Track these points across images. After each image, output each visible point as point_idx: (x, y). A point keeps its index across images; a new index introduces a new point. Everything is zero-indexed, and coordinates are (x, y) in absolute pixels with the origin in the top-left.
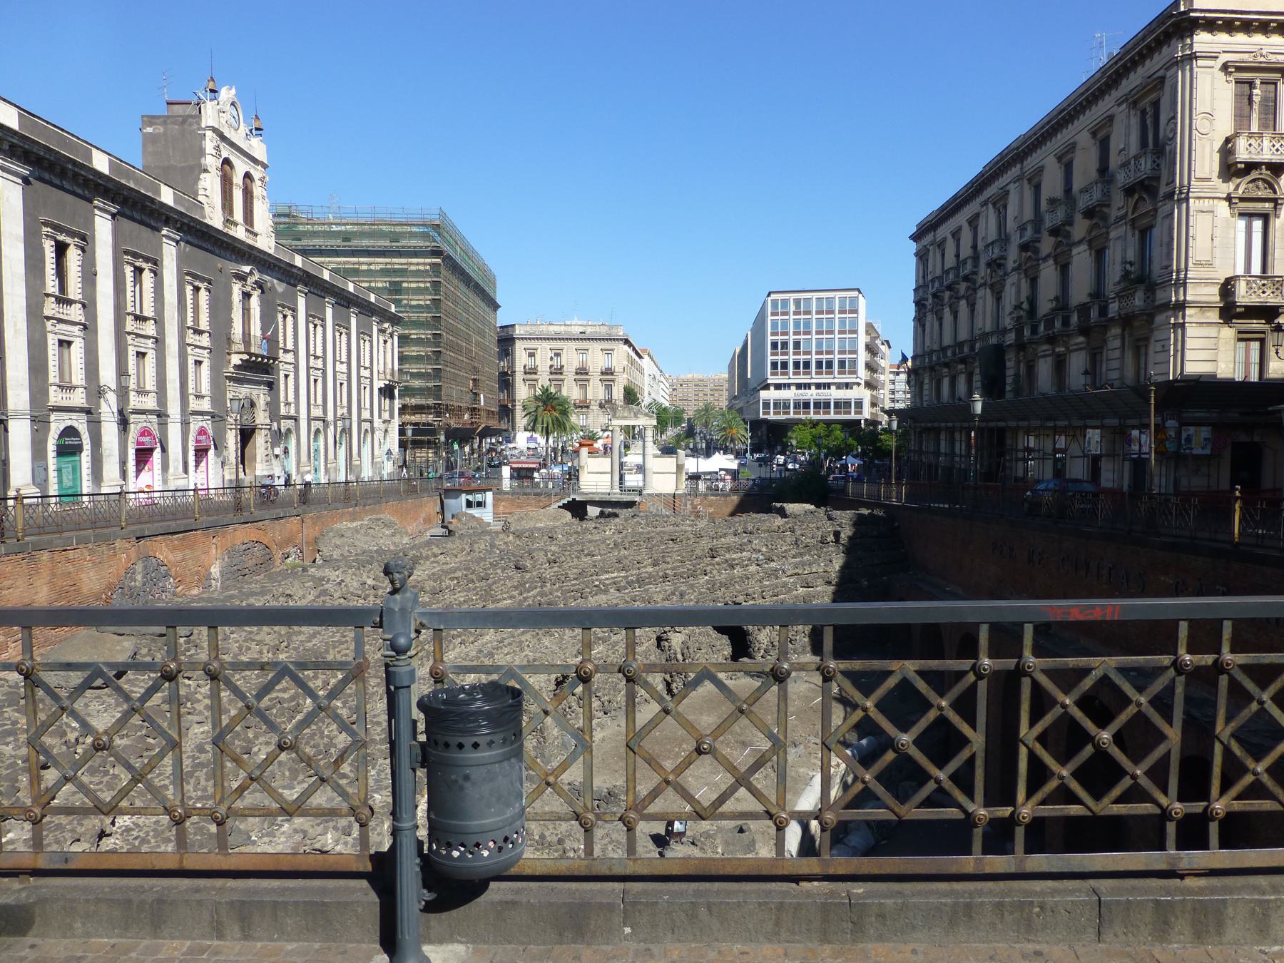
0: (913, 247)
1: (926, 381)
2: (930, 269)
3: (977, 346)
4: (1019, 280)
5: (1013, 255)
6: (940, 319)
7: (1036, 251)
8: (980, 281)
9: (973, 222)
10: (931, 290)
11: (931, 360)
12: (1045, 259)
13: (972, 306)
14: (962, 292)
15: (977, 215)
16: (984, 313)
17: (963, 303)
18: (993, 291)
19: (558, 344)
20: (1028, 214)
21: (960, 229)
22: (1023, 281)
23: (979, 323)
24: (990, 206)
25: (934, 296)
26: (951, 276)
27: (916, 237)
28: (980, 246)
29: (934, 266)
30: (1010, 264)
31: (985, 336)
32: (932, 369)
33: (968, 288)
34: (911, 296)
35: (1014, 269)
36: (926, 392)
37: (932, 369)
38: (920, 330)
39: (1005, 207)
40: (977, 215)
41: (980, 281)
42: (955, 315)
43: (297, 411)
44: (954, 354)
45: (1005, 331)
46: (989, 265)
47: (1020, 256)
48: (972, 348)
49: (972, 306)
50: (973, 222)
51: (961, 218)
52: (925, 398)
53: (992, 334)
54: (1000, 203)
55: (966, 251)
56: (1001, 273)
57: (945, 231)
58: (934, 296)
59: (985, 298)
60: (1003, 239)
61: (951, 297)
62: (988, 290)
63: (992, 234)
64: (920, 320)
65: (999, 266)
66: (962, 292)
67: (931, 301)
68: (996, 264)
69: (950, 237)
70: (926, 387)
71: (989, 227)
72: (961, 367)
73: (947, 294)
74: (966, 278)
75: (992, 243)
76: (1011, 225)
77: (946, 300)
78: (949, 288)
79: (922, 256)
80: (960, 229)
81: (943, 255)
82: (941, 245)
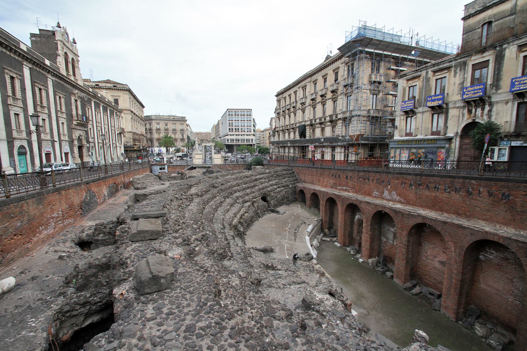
0: (276, 98)
5: (308, 101)
6: (285, 118)
8: (297, 108)
12: (318, 103)
13: (295, 115)
20: (313, 91)
27: (277, 96)
30: (307, 104)
32: (283, 130)
37: (283, 130)
42: (290, 117)
49: (295, 115)
50: (295, 92)
51: (292, 91)
54: (304, 88)
55: (293, 100)
57: (286, 94)
59: (299, 113)
65: (304, 104)
72: (292, 130)
74: (294, 107)
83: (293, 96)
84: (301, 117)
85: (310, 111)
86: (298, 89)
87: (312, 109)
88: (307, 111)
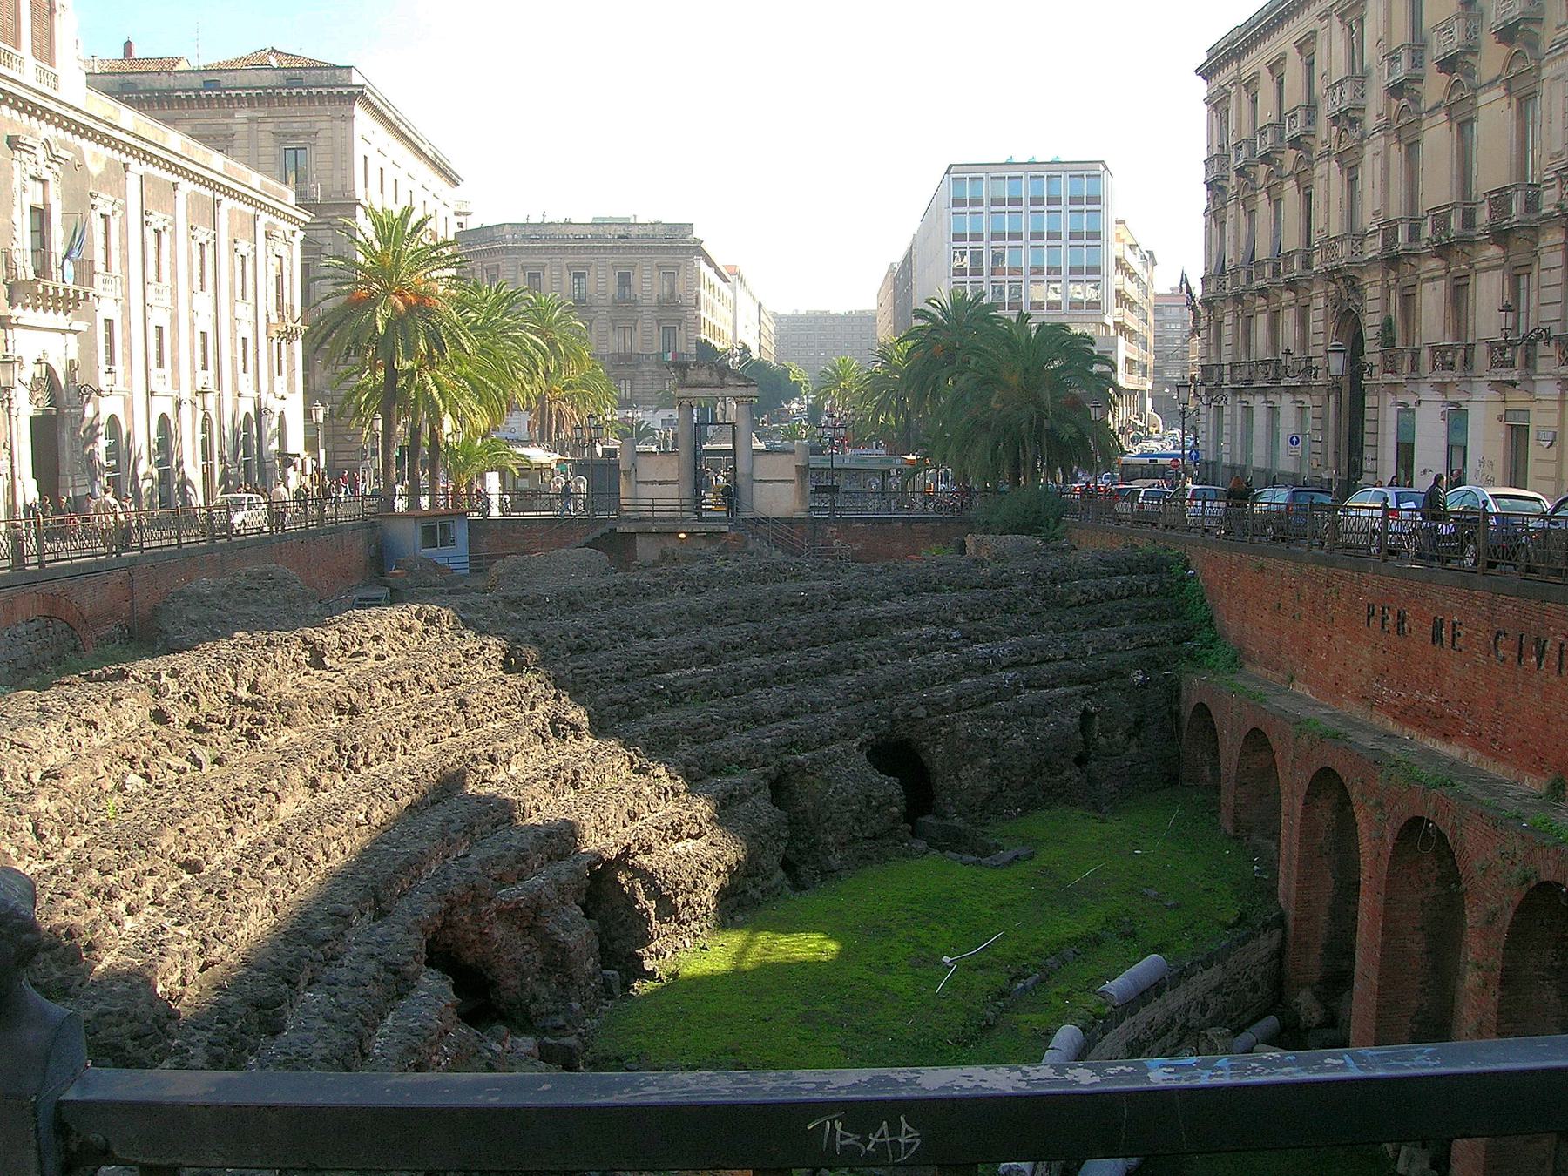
0: (1201, 88)
1: (1228, 320)
2: (1232, 126)
3: (1316, 259)
4: (1387, 148)
5: (1376, 103)
6: (1251, 213)
7: (1416, 100)
9: (1306, 45)
10: (1234, 163)
11: (1235, 283)
14: (1288, 167)
15: (1313, 34)
16: (1328, 202)
17: (1290, 185)
18: (1341, 165)
19: (584, 258)
20: (1401, 35)
21: (1282, 58)
22: (1395, 148)
23: (1318, 223)
24: (1335, 19)
25: (1240, 172)
26: (1269, 138)
27: (1206, 72)
28: (1319, 88)
29: (1239, 120)
30: (1371, 121)
31: (1328, 244)
33: (1299, 160)
34: (1199, 174)
35: (1379, 128)
36: (1226, 340)
37: (1238, 298)
38: (1215, 231)
39: (1361, 21)
40: (1313, 34)
41: (1319, 148)
43: (130, 384)
44: (1276, 273)
45: (1362, 237)
46: (1335, 120)
47: (1389, 105)
48: (1307, 265)
50: (1306, 45)
51: (1285, 41)
52: (1225, 350)
53: (1341, 239)
55: (1294, 96)
56: (1357, 135)
57: (1255, 62)
58: (1240, 172)
59: (1328, 179)
60: (1358, 77)
61: (1269, 175)
62: (1334, 163)
63: (1340, 70)
64: (1215, 216)
65: (1353, 122)
66: (1288, 167)
67: (1234, 181)
68: (1347, 119)
69: (1265, 72)
70: (1227, 330)
71: (1333, 57)
72: (1287, 296)
73: (1263, 168)
74: (1295, 143)
75: (1340, 82)
76: (1371, 53)
77: (1261, 181)
78: (1266, 158)
79: (1217, 104)
80: (1282, 58)
81: (1254, 102)
82: (1250, 85)
83: (1294, 71)
84: (1334, 204)
85: (1386, 168)
86: (1319, 26)
87: (1397, 155)
88: (1370, 170)
